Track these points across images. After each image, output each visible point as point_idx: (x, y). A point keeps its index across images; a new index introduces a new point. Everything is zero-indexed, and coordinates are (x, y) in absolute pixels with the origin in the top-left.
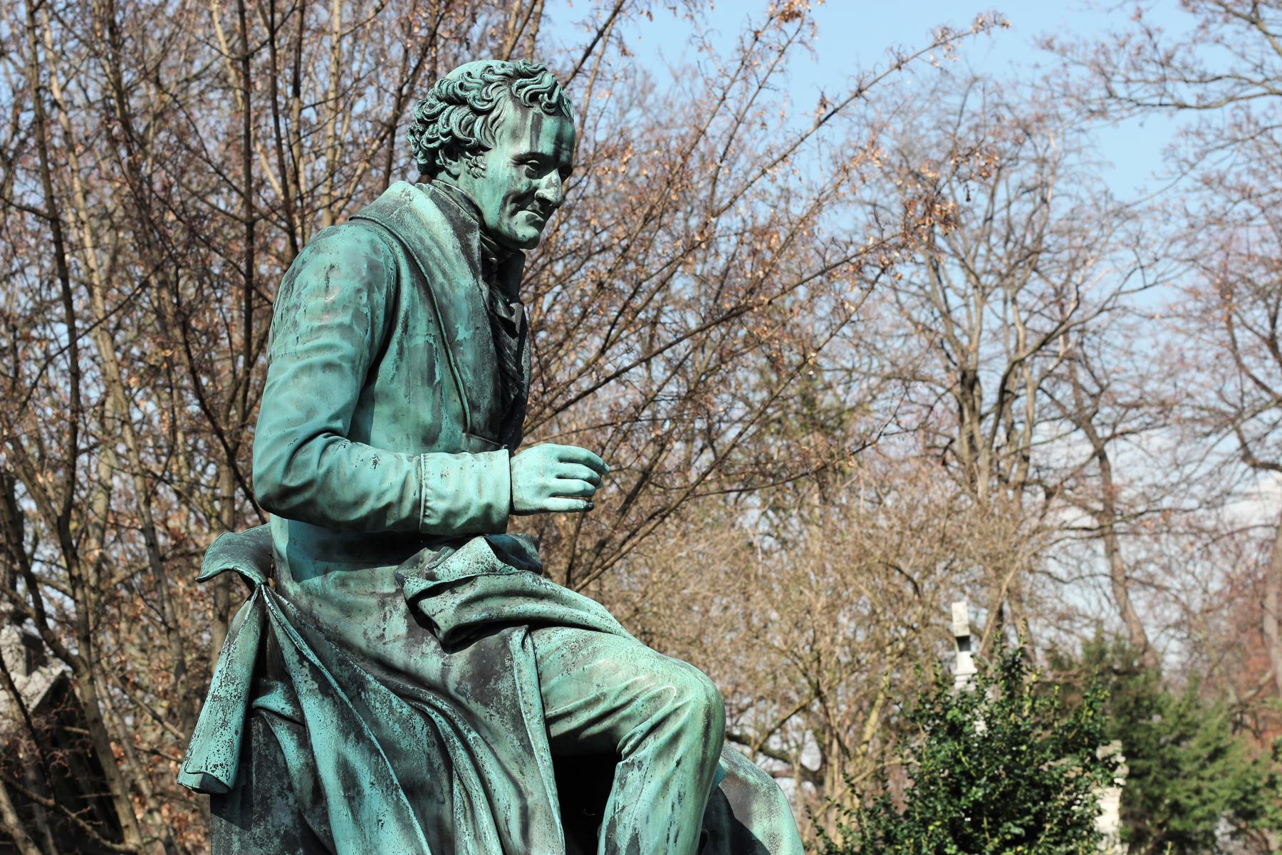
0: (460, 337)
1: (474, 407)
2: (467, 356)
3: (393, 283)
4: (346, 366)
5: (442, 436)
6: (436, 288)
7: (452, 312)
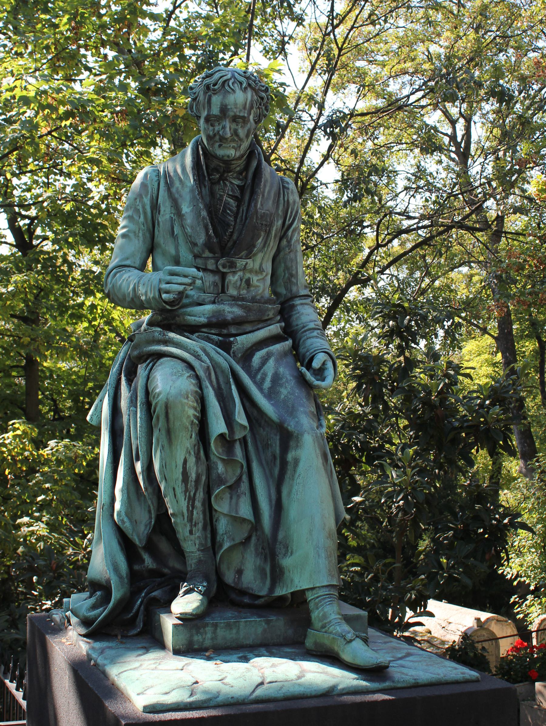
0: (183, 212)
1: (195, 244)
2: (189, 220)
3: (156, 192)
4: (131, 235)
5: (181, 260)
6: (174, 190)
7: (180, 201)
